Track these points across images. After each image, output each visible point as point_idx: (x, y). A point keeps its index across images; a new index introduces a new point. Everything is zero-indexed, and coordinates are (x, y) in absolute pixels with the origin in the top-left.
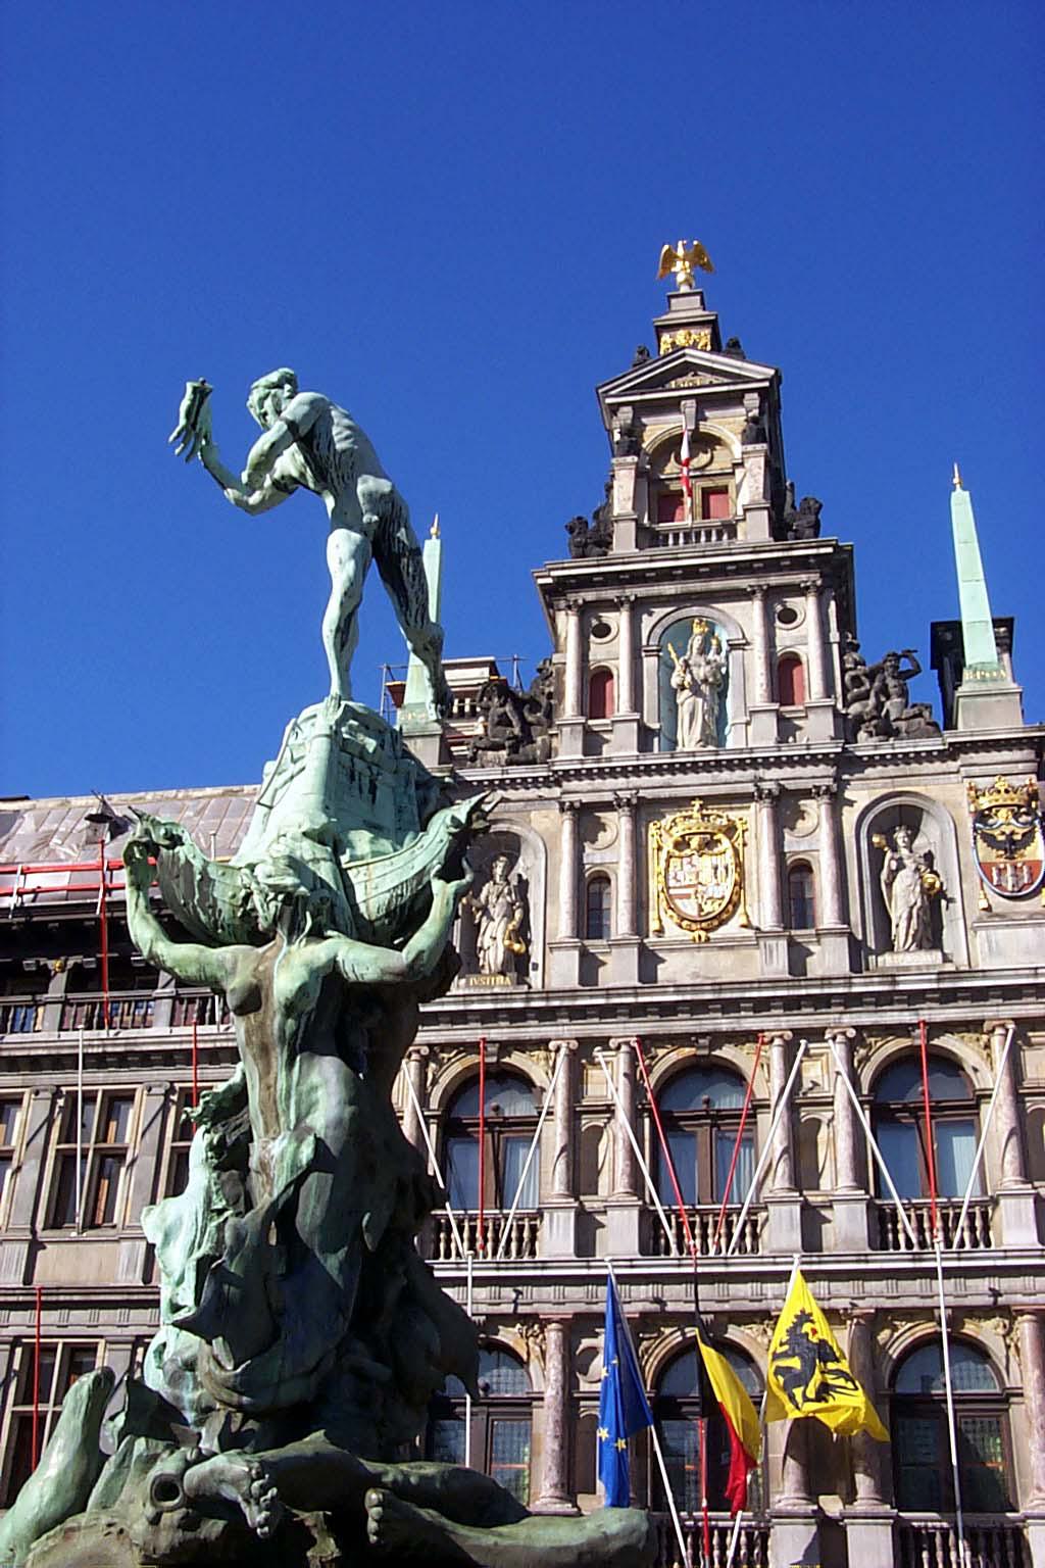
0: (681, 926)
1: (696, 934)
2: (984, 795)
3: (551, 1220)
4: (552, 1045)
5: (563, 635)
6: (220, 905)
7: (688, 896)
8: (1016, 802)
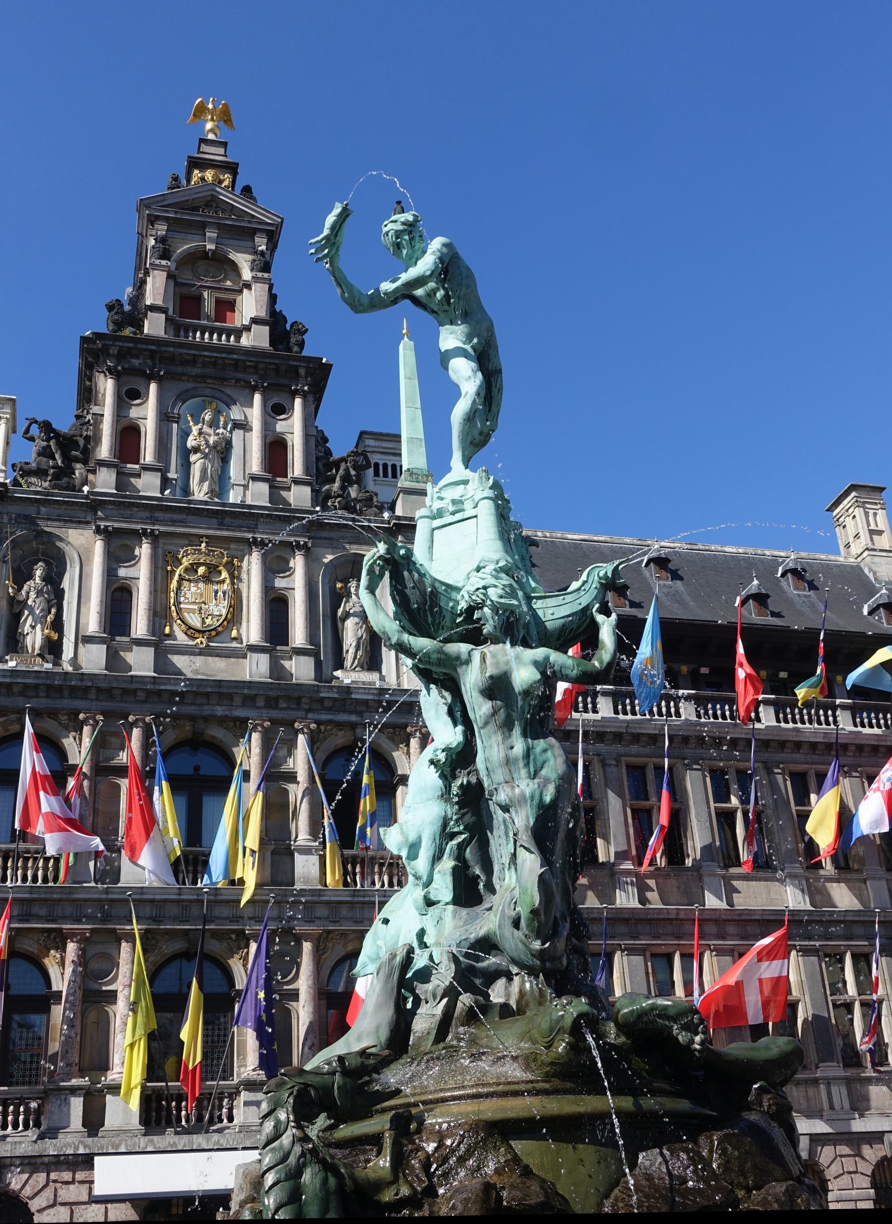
1: (198, 641)
5: (102, 391)
6: (444, 612)
7: (194, 612)
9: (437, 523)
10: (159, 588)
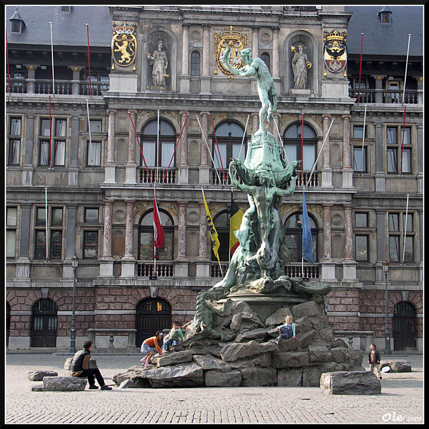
0: (224, 73)
1: (230, 76)
2: (329, 35)
3: (181, 172)
4: (181, 113)
8: (339, 39)
9: (253, 147)
10: (211, 52)
